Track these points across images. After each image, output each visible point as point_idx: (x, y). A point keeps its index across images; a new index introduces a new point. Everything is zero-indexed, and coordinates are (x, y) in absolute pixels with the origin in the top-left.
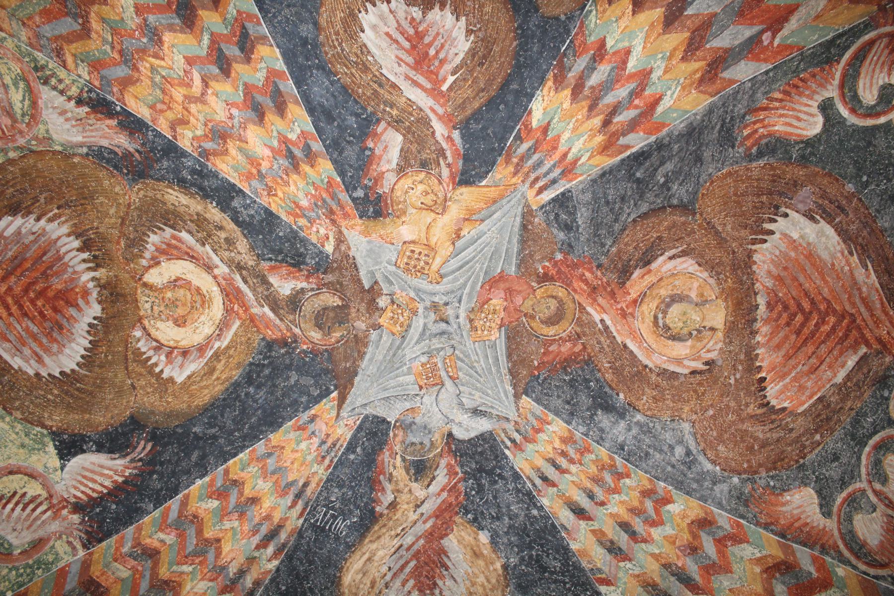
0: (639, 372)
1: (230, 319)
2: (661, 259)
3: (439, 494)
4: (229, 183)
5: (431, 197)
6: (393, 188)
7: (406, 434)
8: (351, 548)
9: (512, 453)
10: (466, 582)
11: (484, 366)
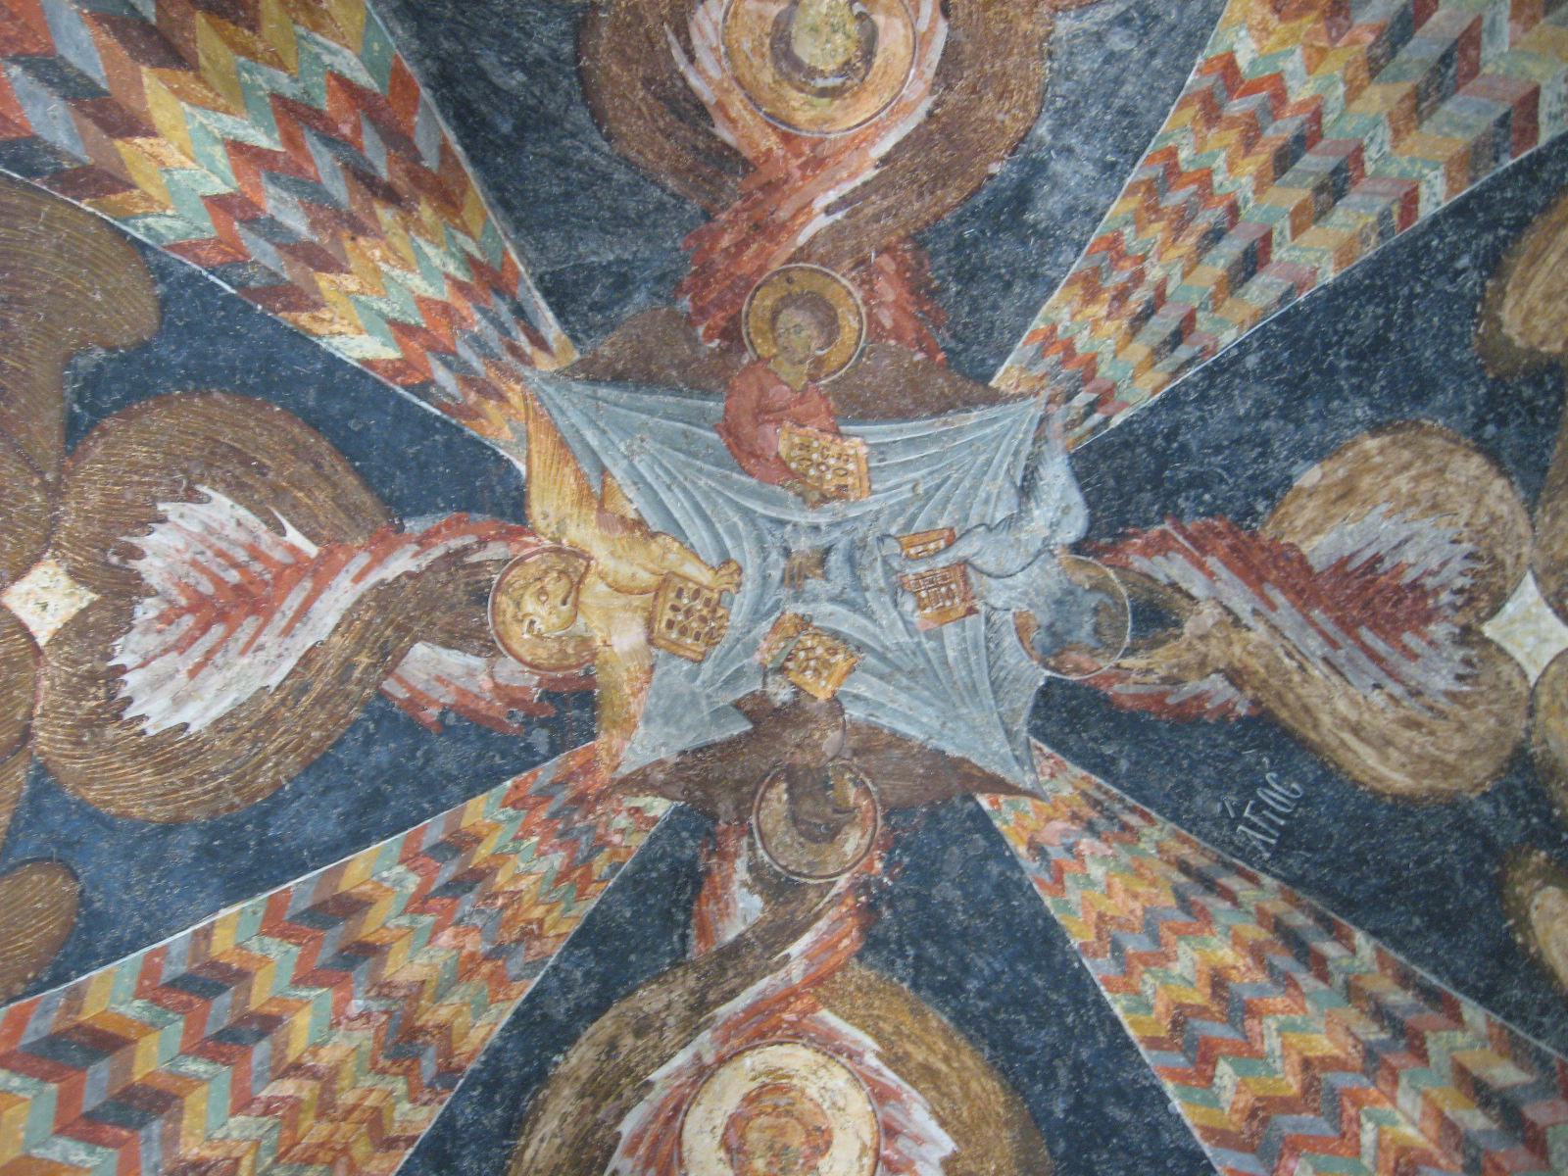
0: (942, 131)
1: (815, 1029)
2: (694, 81)
3: (1211, 575)
4: (512, 1024)
5: (550, 583)
6: (530, 665)
7: (1076, 647)
8: (1329, 772)
10: (1409, 515)
11: (924, 472)
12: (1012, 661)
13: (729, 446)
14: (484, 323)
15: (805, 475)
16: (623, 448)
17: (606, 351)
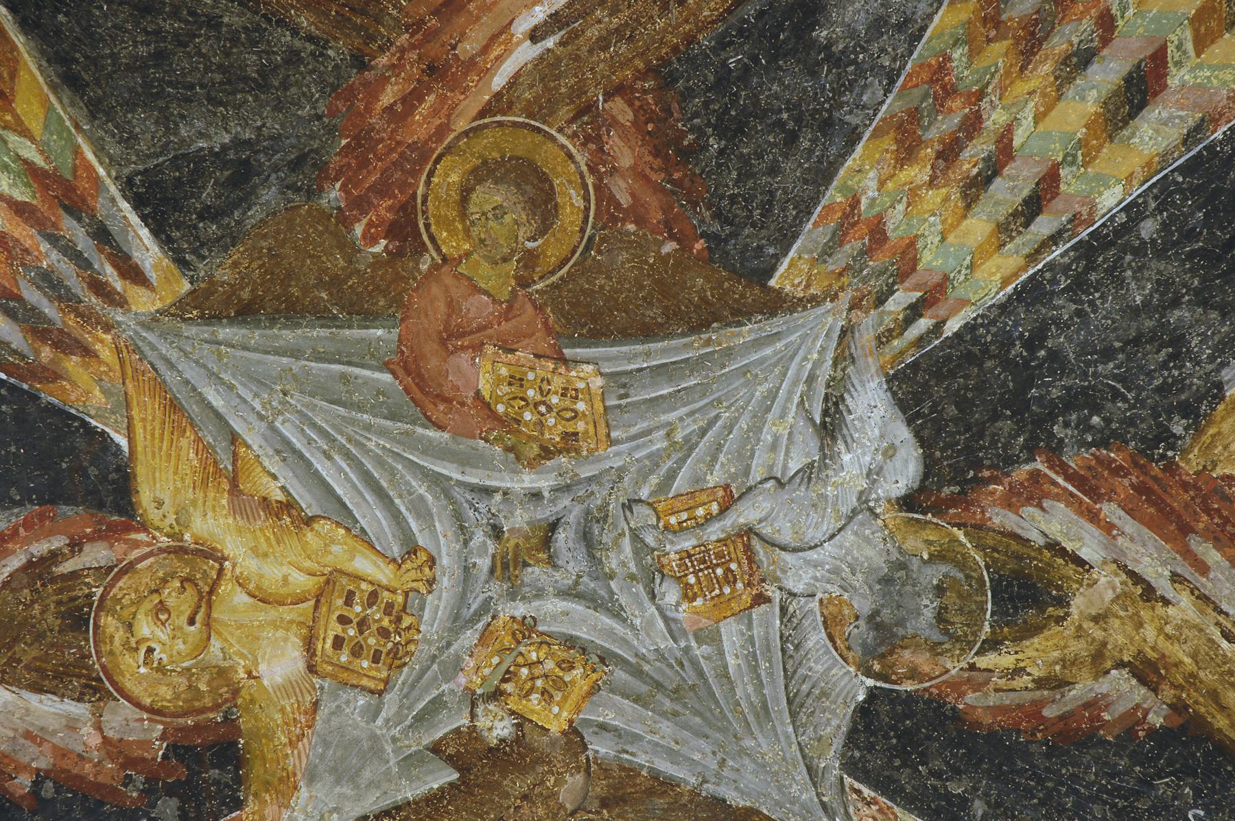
3: (1108, 528)
5: (170, 594)
6: (151, 710)
7: (912, 642)
9: (953, 312)
12: (819, 668)
13: (407, 390)
14: (55, 255)
15: (518, 422)
16: (258, 407)
17: (224, 275)
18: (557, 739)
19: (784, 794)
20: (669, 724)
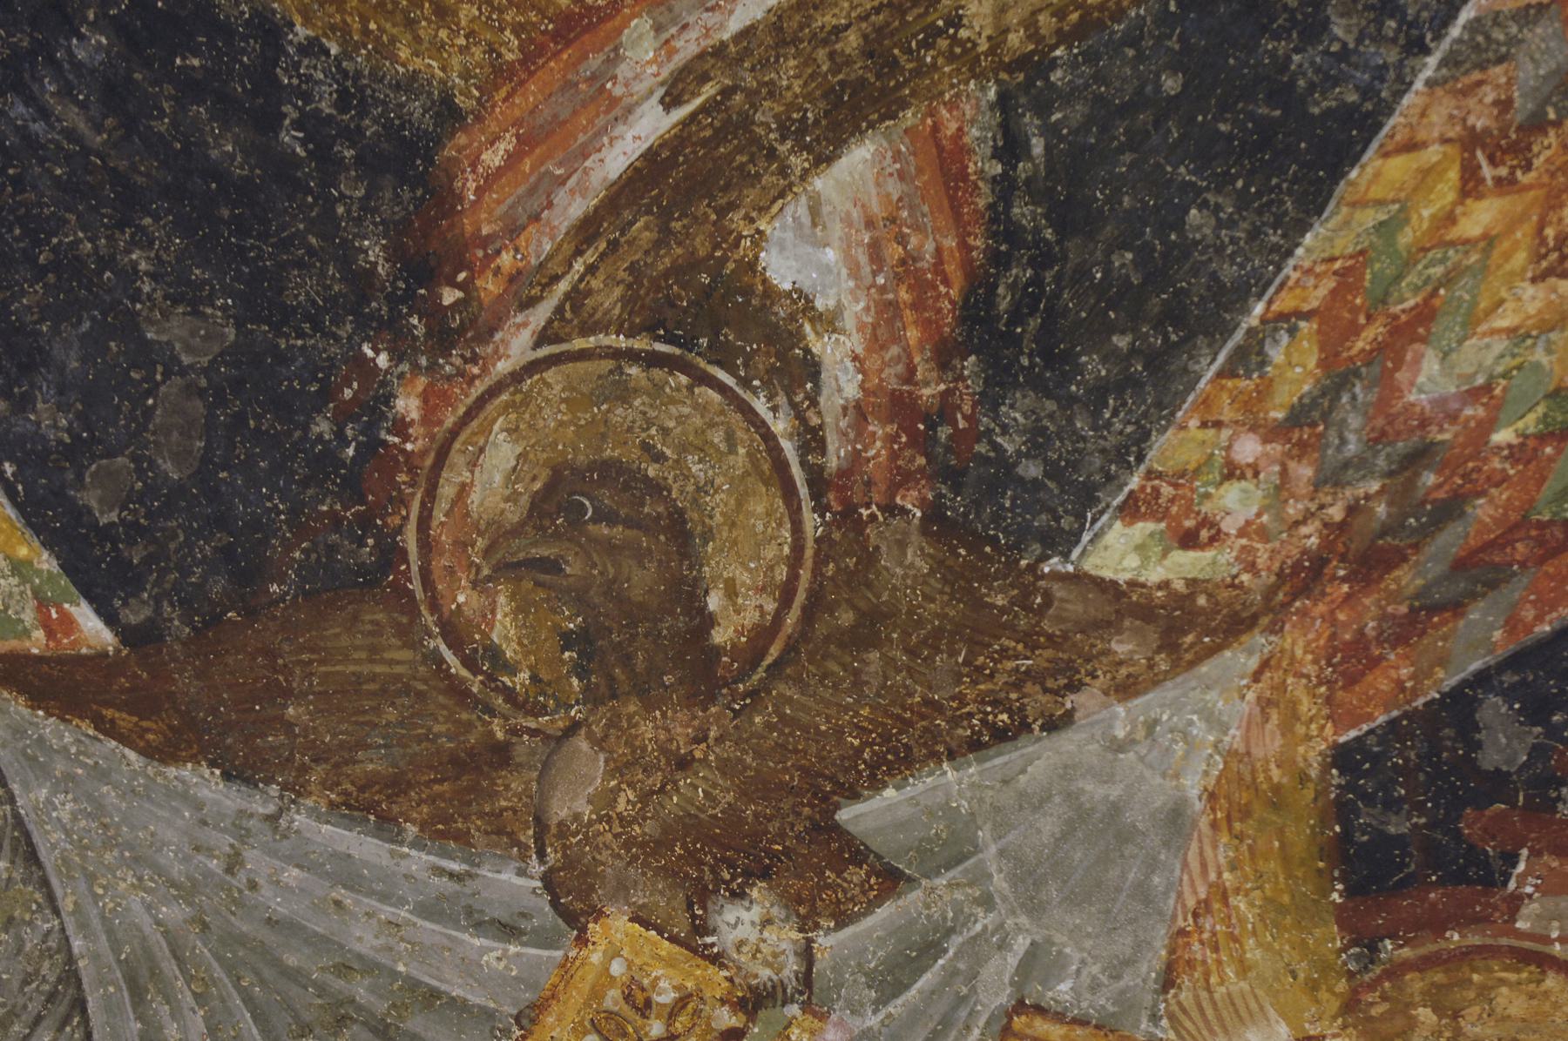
18: (613, 898)
19: (90, 798)
20: (358, 947)
